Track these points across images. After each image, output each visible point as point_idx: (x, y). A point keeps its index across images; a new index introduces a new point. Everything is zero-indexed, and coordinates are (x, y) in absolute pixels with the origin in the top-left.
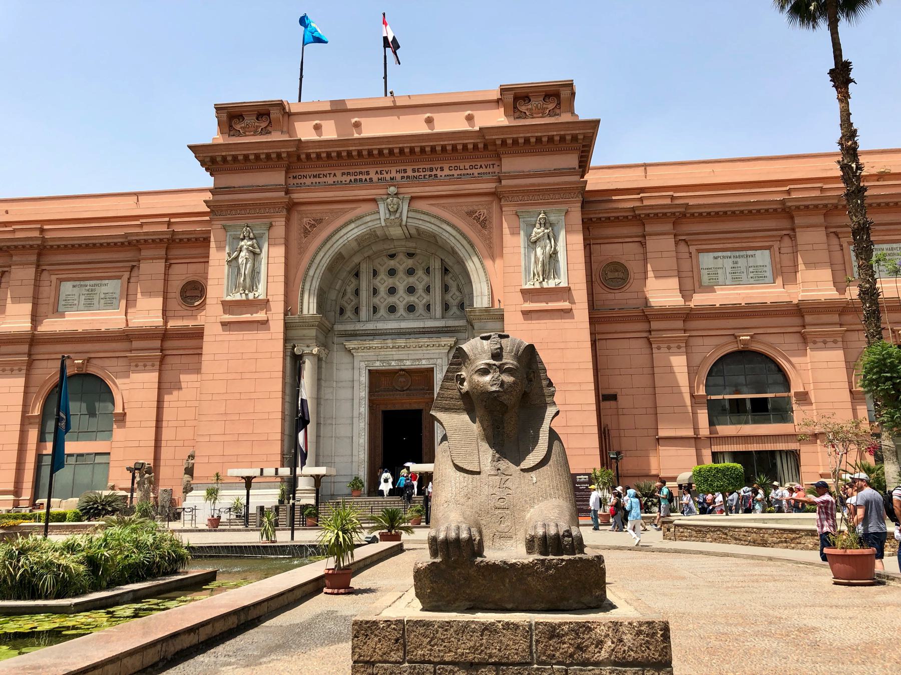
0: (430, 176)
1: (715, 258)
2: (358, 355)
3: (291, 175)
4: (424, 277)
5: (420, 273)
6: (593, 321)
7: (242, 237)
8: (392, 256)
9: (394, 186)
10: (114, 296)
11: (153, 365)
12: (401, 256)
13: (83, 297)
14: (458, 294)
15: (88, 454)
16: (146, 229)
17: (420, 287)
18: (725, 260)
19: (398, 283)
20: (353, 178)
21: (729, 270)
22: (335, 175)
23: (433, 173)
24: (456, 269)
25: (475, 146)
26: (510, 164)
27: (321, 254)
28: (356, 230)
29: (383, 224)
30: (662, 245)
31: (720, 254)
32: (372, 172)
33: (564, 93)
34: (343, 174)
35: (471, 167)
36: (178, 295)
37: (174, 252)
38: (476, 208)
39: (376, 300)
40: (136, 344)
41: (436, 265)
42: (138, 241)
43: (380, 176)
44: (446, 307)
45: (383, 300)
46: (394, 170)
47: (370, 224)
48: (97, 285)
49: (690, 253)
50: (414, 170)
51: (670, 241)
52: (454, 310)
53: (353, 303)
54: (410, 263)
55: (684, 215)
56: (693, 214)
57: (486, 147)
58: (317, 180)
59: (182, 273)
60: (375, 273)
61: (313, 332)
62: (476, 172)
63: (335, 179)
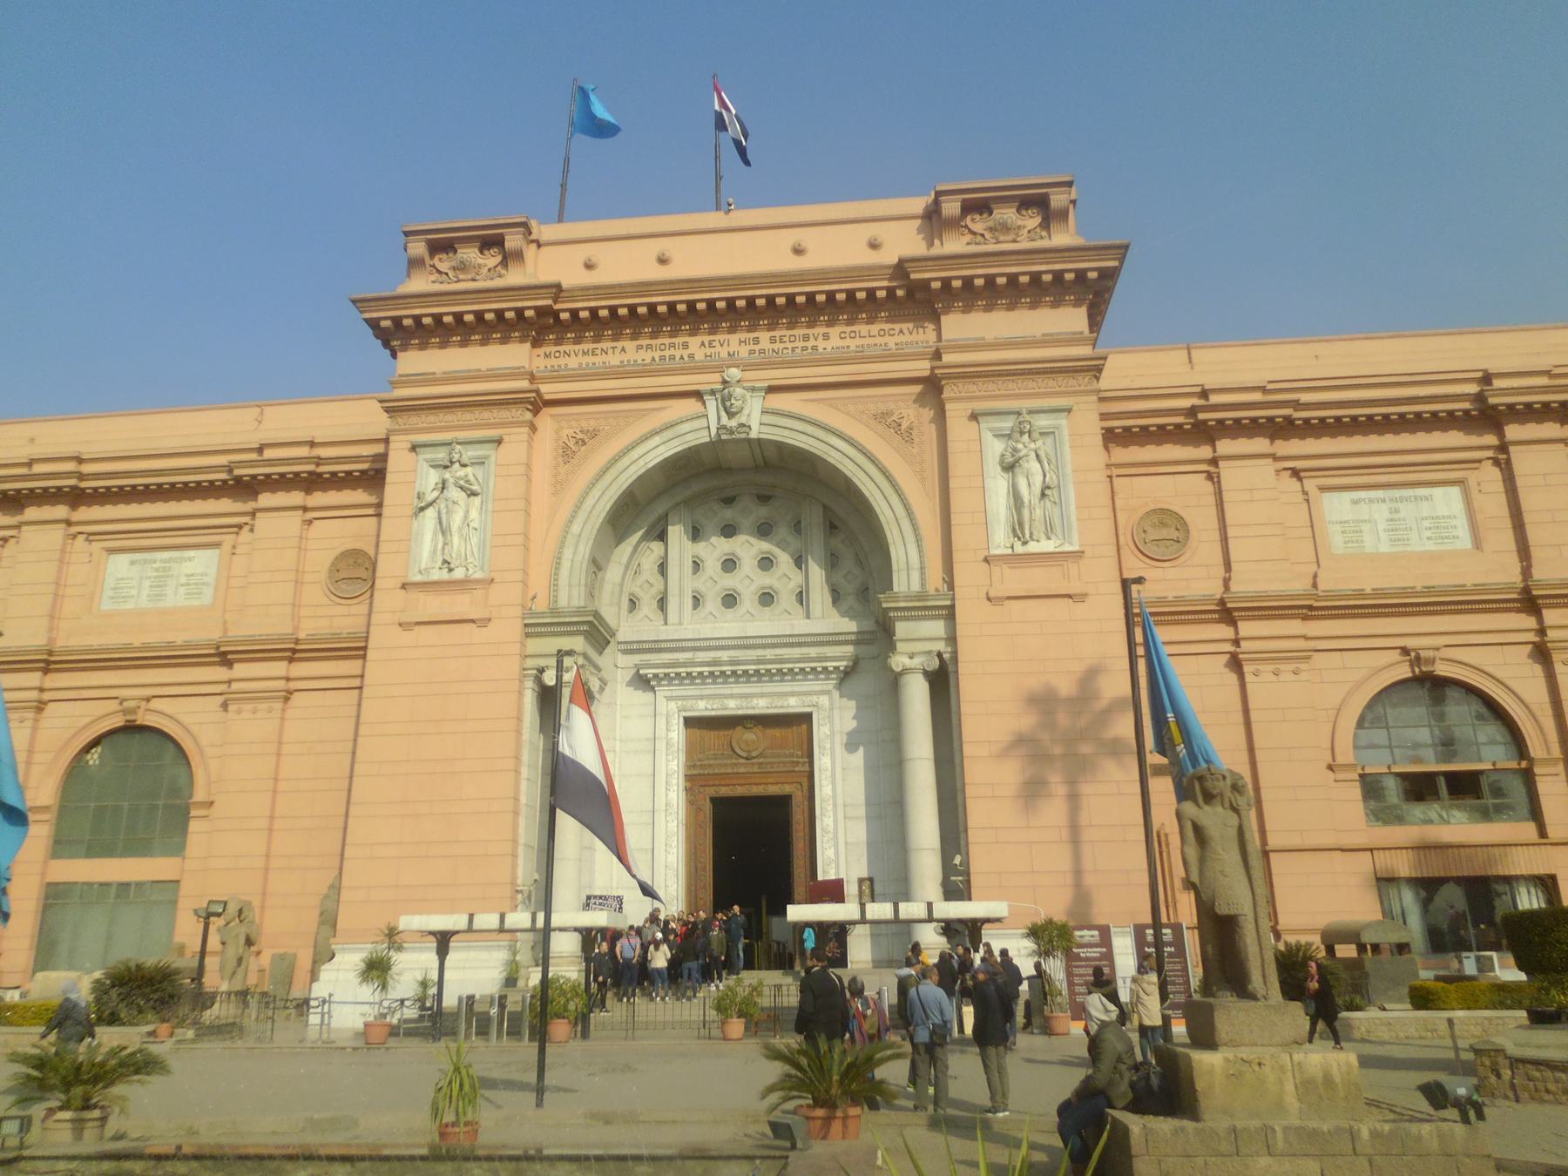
0: (804, 349)
1: (1355, 502)
3: (541, 351)
8: (729, 501)
9: (737, 366)
10: (206, 579)
13: (147, 583)
15: (139, 885)
18: (1375, 506)
19: (739, 552)
20: (657, 355)
21: (1382, 526)
22: (623, 349)
23: (811, 343)
25: (891, 291)
26: (959, 325)
27: (596, 492)
28: (662, 449)
30: (1251, 474)
31: (1363, 494)
32: (694, 342)
34: (639, 347)
35: (882, 333)
36: (324, 575)
37: (319, 498)
38: (892, 406)
39: (700, 583)
40: (240, 670)
41: (813, 518)
42: (254, 477)
43: (709, 351)
45: (714, 582)
46: (734, 338)
47: (689, 437)
49: (1305, 493)
50: (773, 340)
51: (1267, 468)
52: (850, 601)
54: (762, 512)
55: (1289, 421)
56: (1307, 421)
57: (912, 296)
58: (590, 359)
60: (696, 534)
62: (891, 342)
63: (625, 358)
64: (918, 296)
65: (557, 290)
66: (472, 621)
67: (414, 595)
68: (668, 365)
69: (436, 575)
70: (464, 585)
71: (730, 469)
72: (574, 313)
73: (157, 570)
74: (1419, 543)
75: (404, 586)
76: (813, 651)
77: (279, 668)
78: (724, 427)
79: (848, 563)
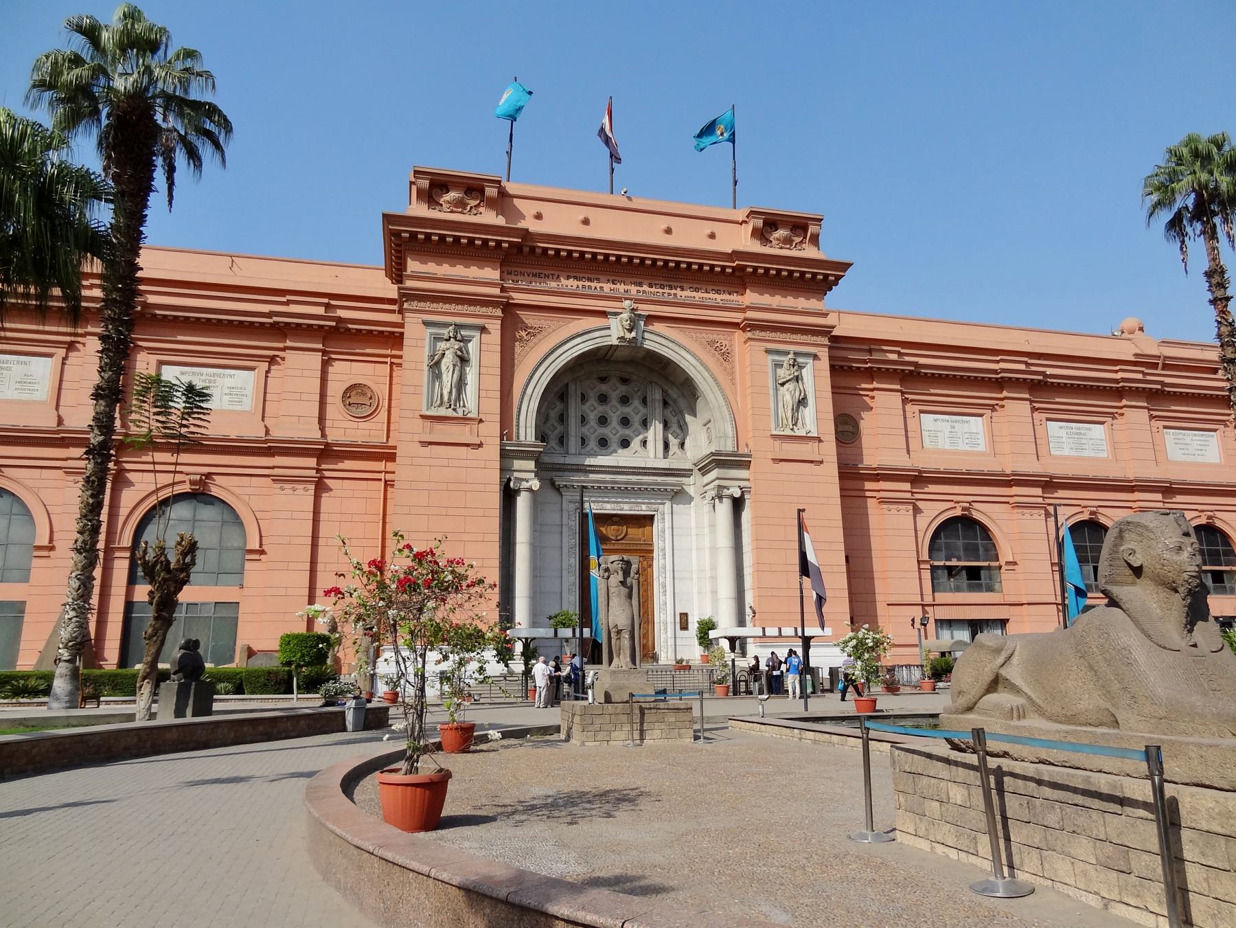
0: (669, 294)
2: (568, 495)
3: (505, 269)
4: (641, 408)
5: (636, 403)
6: (843, 476)
7: (446, 337)
8: (603, 380)
11: (306, 490)
12: (614, 381)
14: (679, 431)
16: (293, 308)
17: (636, 420)
20: (580, 284)
21: (947, 434)
24: (682, 403)
29: (616, 342)
33: (812, 229)
34: (568, 278)
38: (716, 337)
39: (584, 430)
41: (658, 396)
44: (666, 446)
45: (594, 431)
47: (598, 340)
48: (219, 375)
53: (556, 432)
54: (622, 389)
59: (344, 372)
61: (531, 465)
62: (719, 297)
64: (737, 273)
65: (525, 233)
66: (467, 445)
67: (428, 423)
68: (587, 292)
69: (443, 412)
70: (465, 419)
71: (609, 361)
72: (533, 249)
73: (204, 381)
74: (962, 447)
75: (423, 417)
76: (660, 479)
77: (312, 462)
78: (623, 338)
79: (674, 427)
